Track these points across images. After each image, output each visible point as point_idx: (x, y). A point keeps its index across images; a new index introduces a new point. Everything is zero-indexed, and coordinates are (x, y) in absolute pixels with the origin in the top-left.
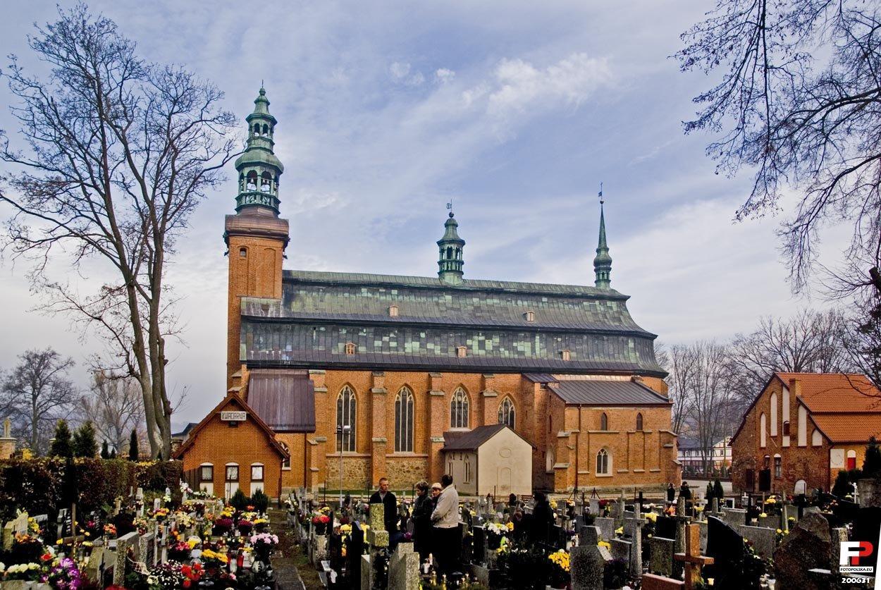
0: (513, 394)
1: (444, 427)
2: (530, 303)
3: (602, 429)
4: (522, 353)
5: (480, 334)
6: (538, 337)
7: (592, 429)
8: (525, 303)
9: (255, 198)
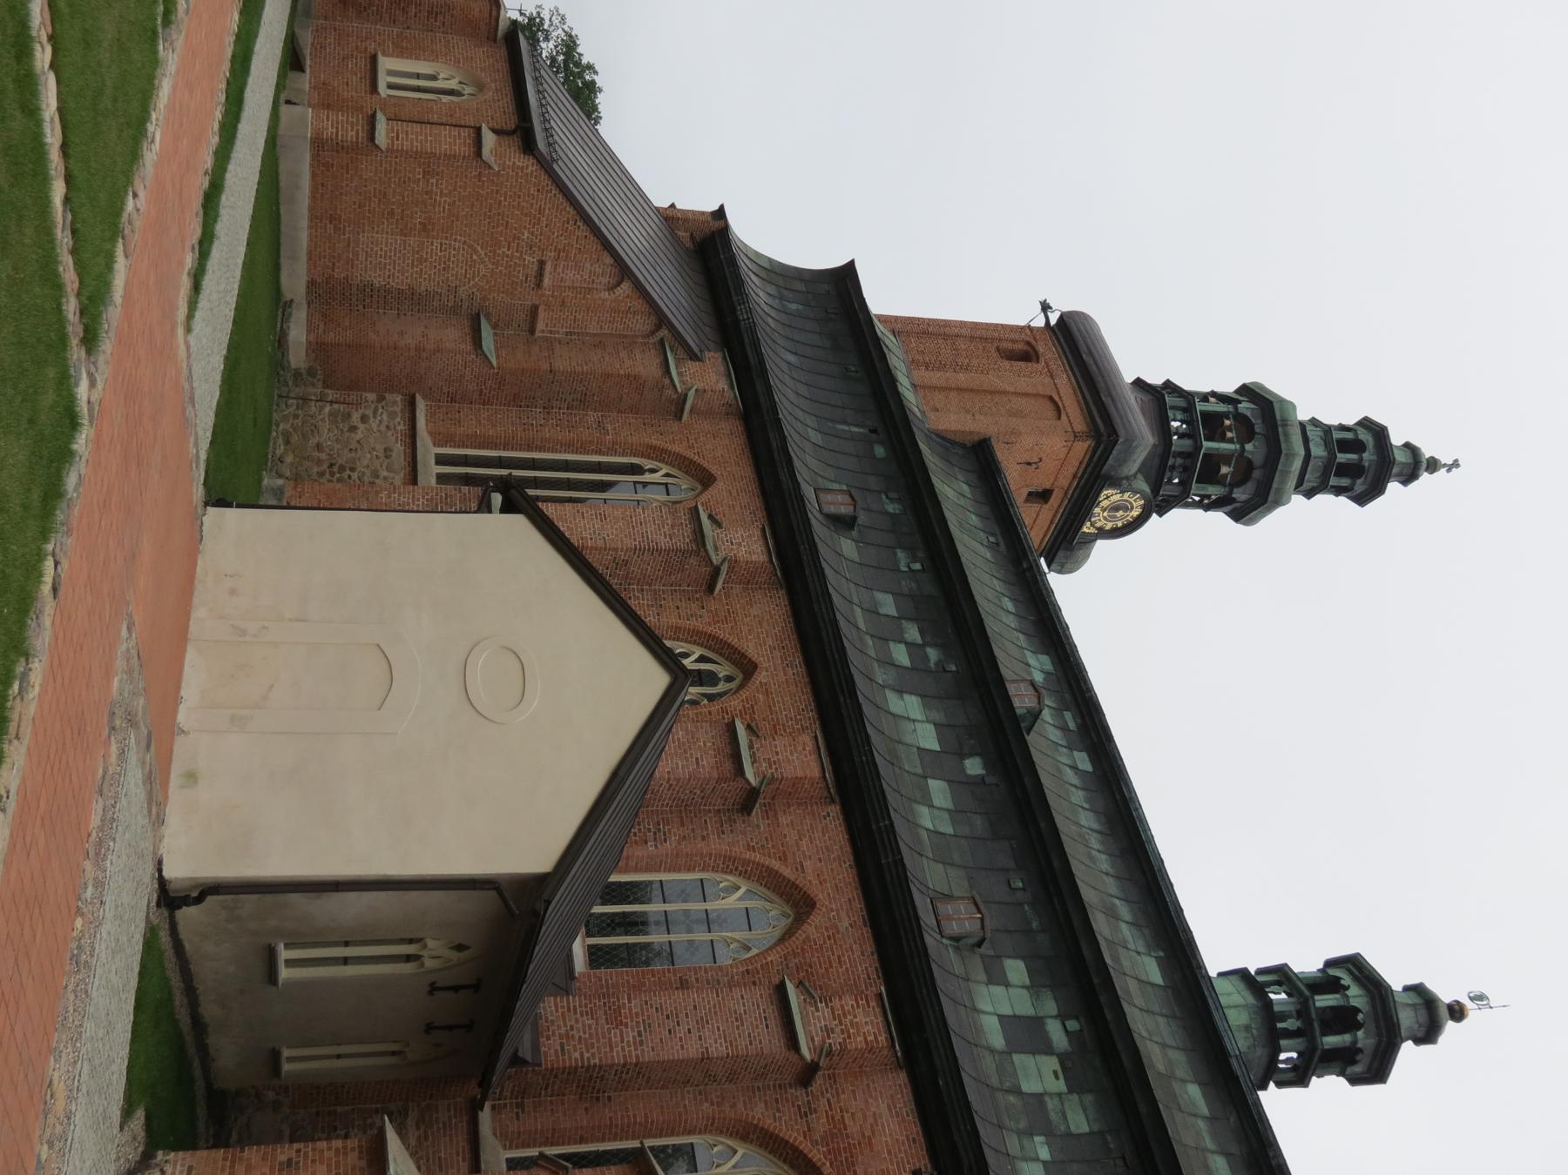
5: (1073, 1025)
9: (1182, 436)
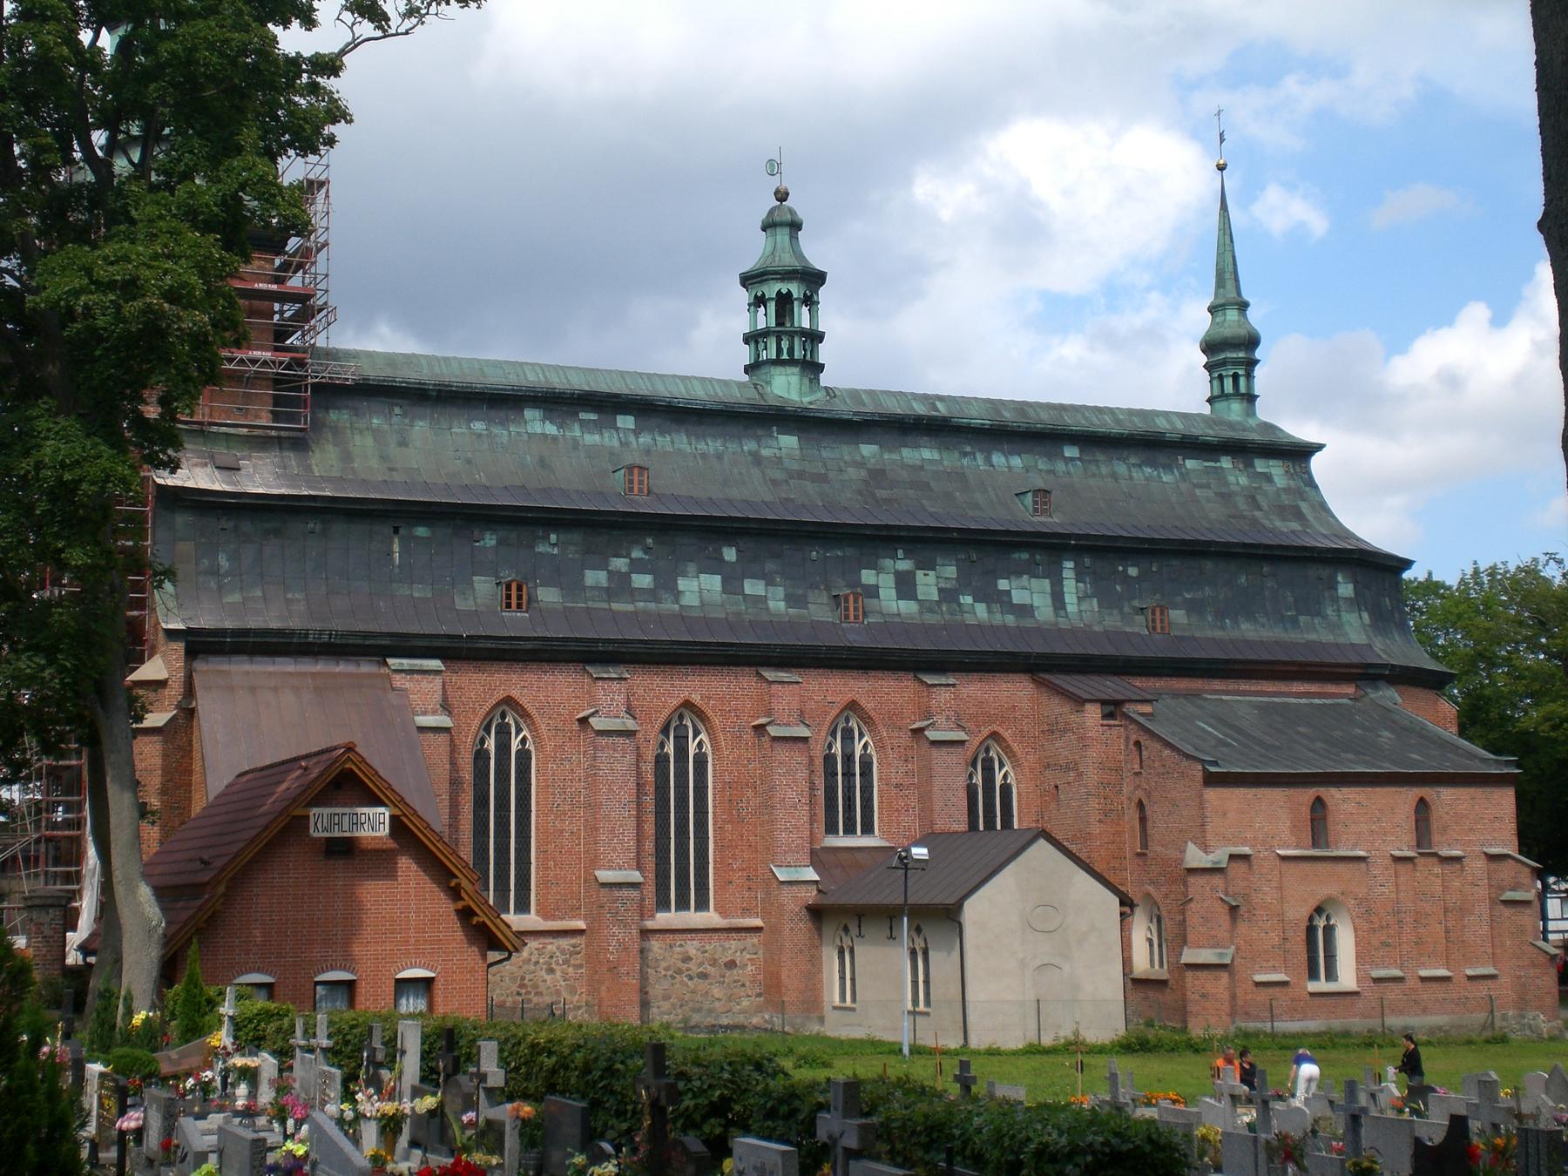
0: (1006, 734)
2: (1029, 459)
3: (1315, 844)
4: (1026, 610)
5: (900, 553)
7: (1288, 847)
8: (1016, 461)
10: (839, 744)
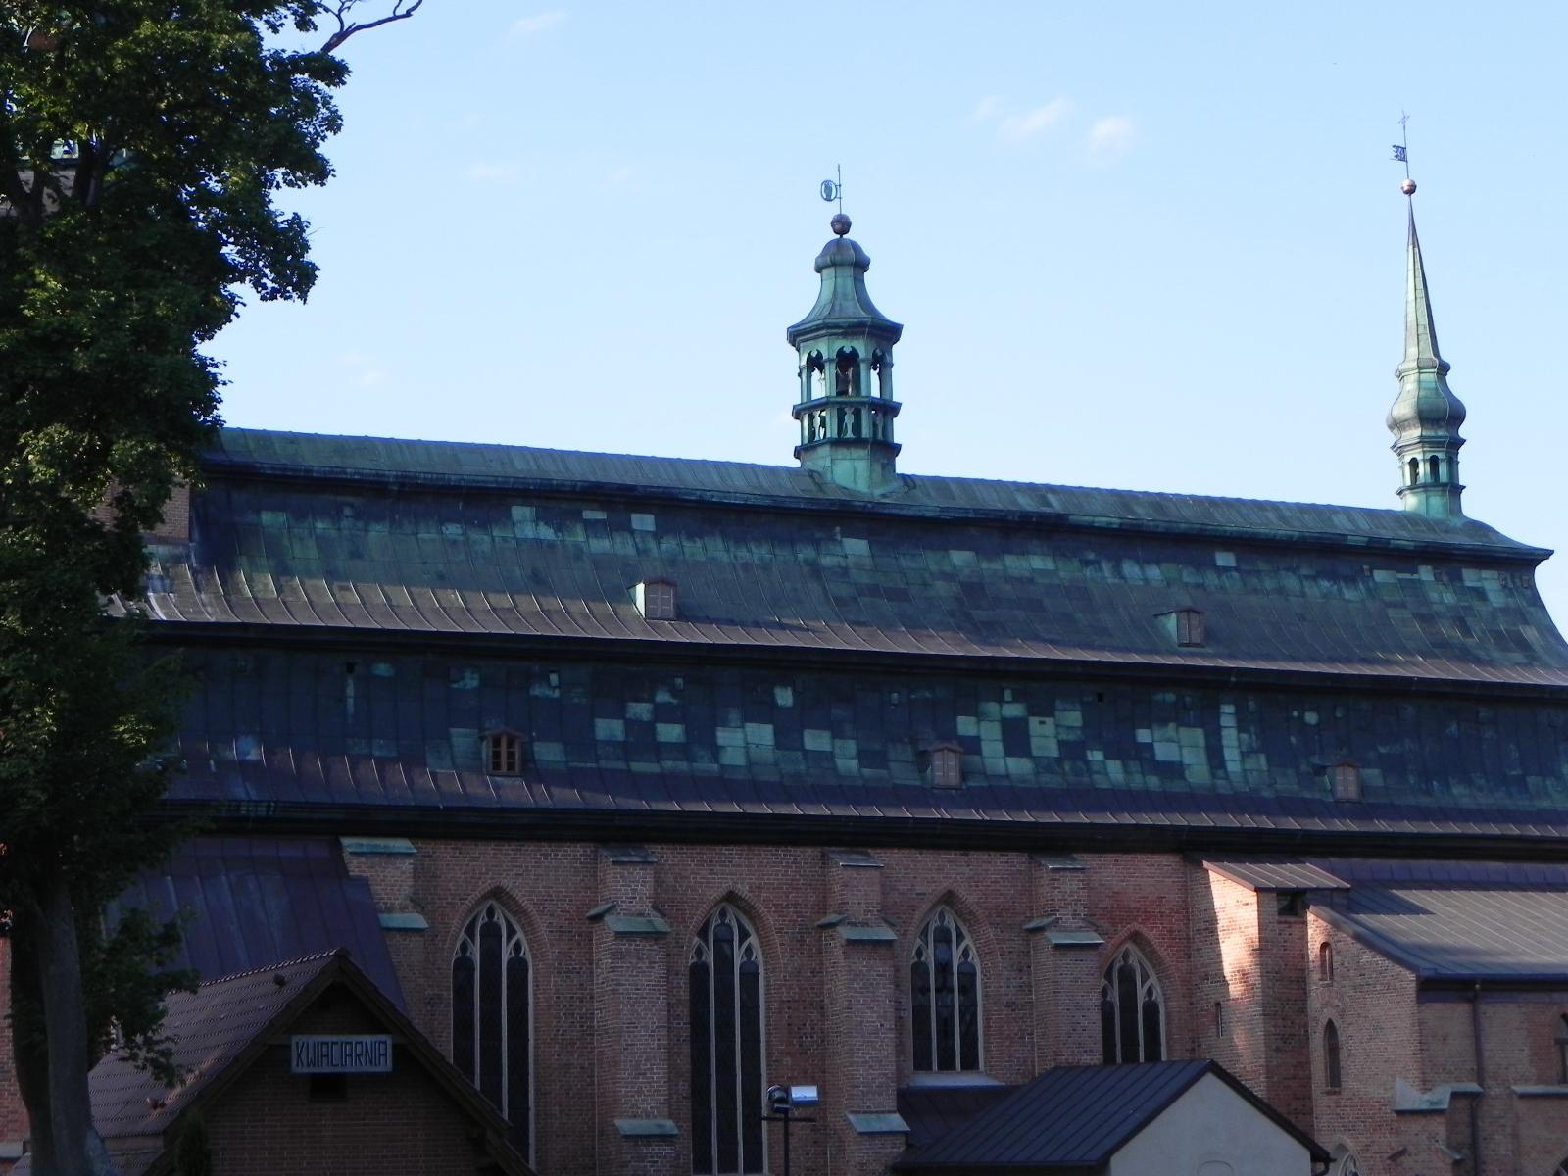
0: (1152, 935)
1: (899, 1070)
2: (1170, 569)
4: (1174, 770)
5: (1008, 694)
6: (1228, 709)
7: (1526, 1081)
8: (1154, 573)
10: (931, 949)
